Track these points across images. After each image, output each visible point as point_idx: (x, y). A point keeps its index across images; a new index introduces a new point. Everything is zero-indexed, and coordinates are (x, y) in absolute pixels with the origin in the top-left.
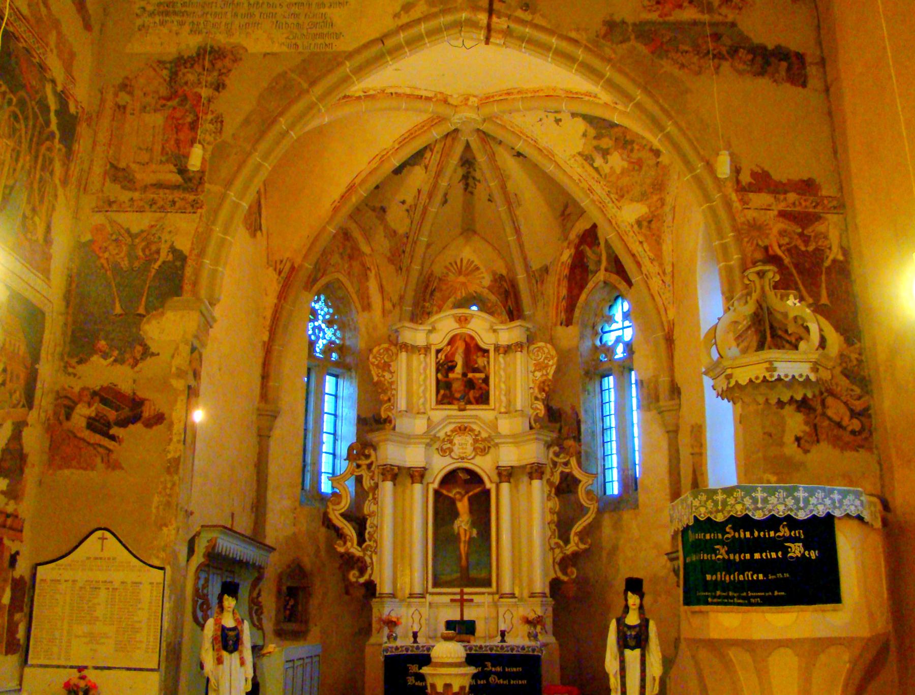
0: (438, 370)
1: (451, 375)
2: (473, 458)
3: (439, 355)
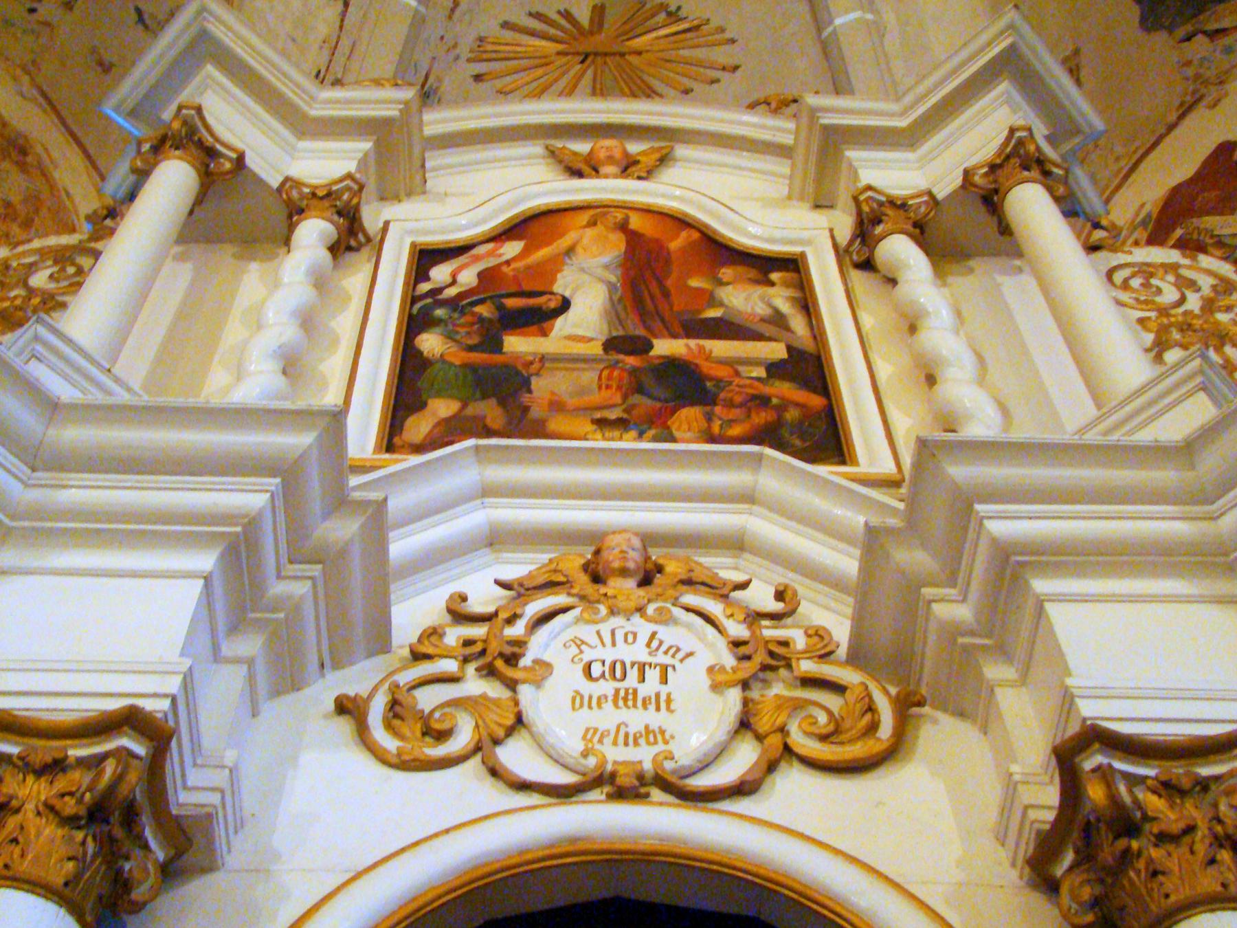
0: (414, 322)
1: (517, 344)
2: (742, 789)
3: (440, 273)
